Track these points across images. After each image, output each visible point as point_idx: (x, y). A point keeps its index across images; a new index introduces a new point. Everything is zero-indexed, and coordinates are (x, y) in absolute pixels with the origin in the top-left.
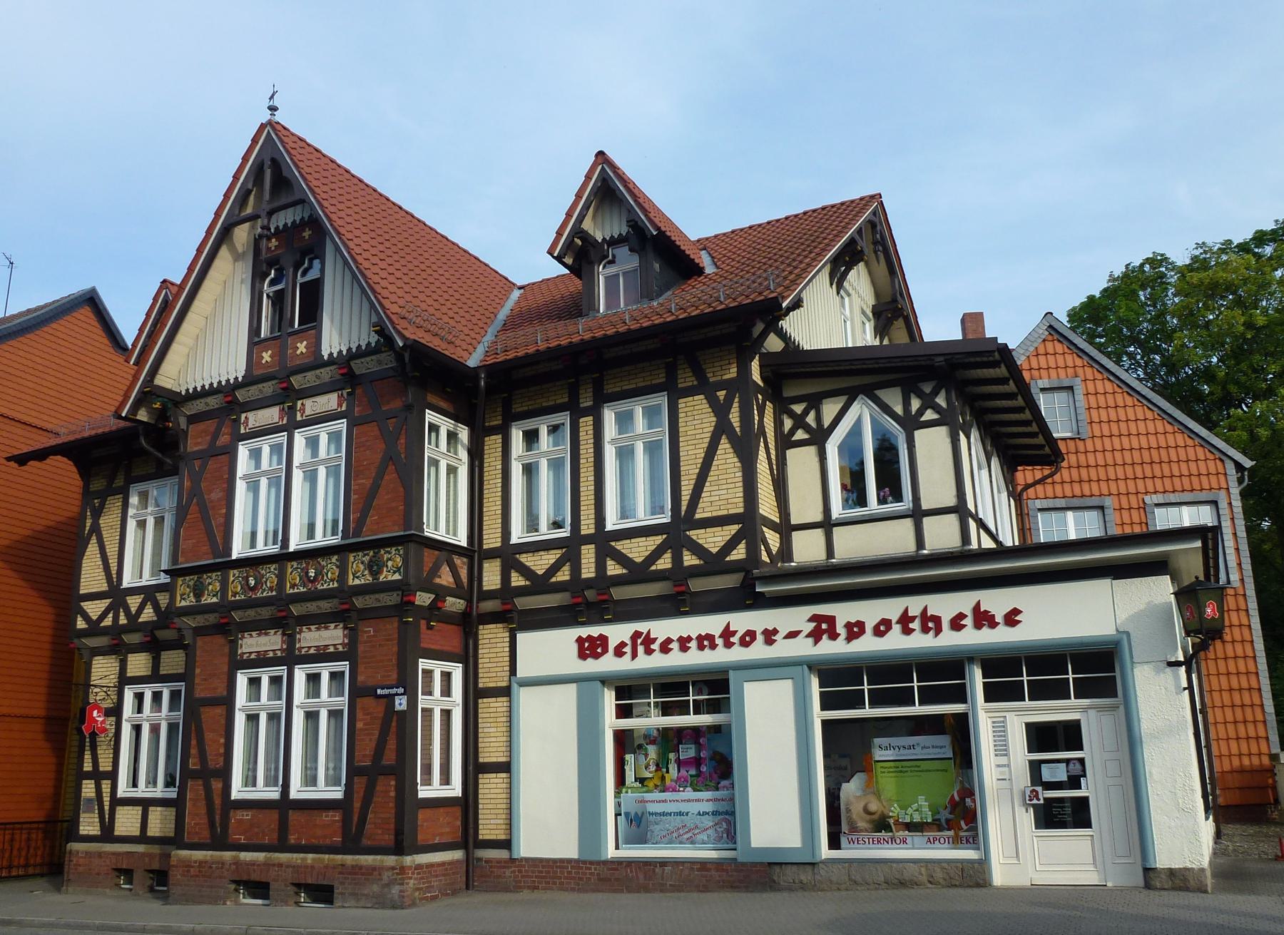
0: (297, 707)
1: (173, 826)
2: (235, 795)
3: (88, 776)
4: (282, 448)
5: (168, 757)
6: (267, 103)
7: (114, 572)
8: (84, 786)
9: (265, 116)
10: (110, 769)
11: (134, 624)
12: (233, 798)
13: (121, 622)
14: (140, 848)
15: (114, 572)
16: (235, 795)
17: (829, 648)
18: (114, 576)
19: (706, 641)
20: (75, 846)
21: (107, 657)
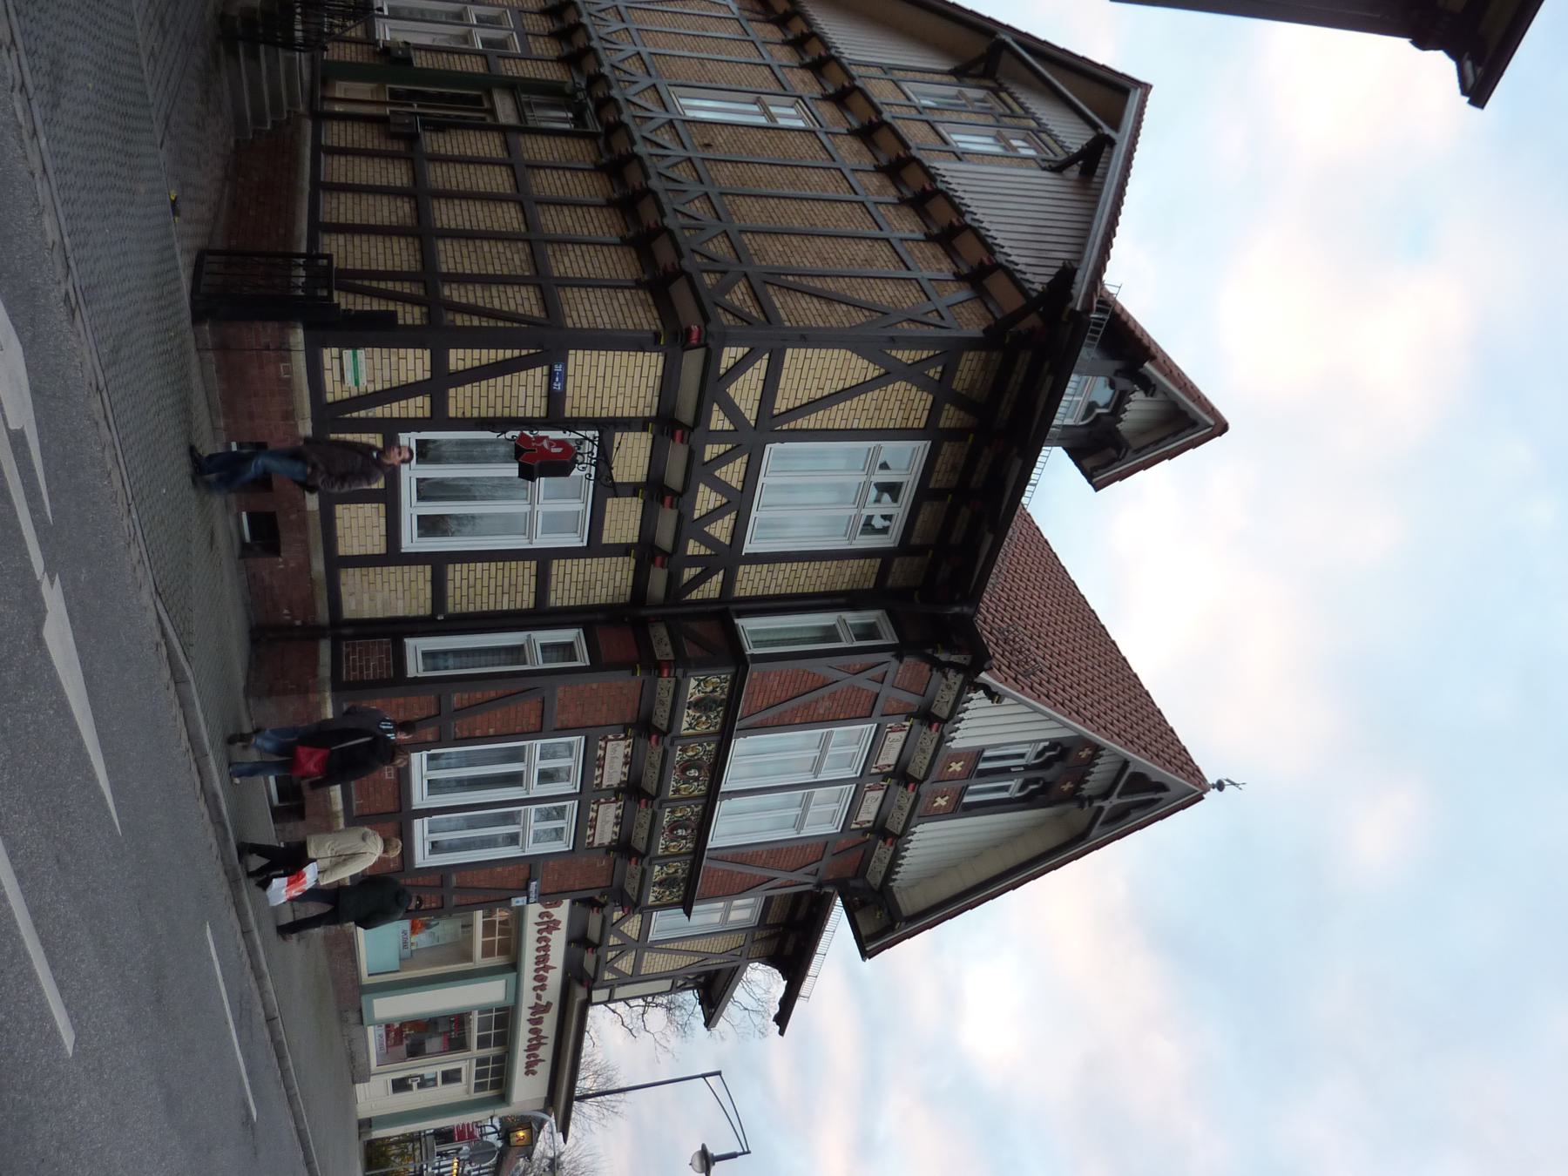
0: (529, 636)
1: (356, 553)
2: (410, 642)
3: (439, 362)
4: (874, 638)
5: (457, 653)
6: (1223, 777)
7: (802, 423)
8: (419, 352)
9: (1211, 779)
10: (452, 413)
11: (696, 470)
12: (406, 640)
13: (691, 543)
14: (318, 566)
15: (802, 423)
16: (410, 642)
17: (525, 1014)
18: (792, 425)
19: (542, 961)
20: (298, 337)
21: (658, 382)
